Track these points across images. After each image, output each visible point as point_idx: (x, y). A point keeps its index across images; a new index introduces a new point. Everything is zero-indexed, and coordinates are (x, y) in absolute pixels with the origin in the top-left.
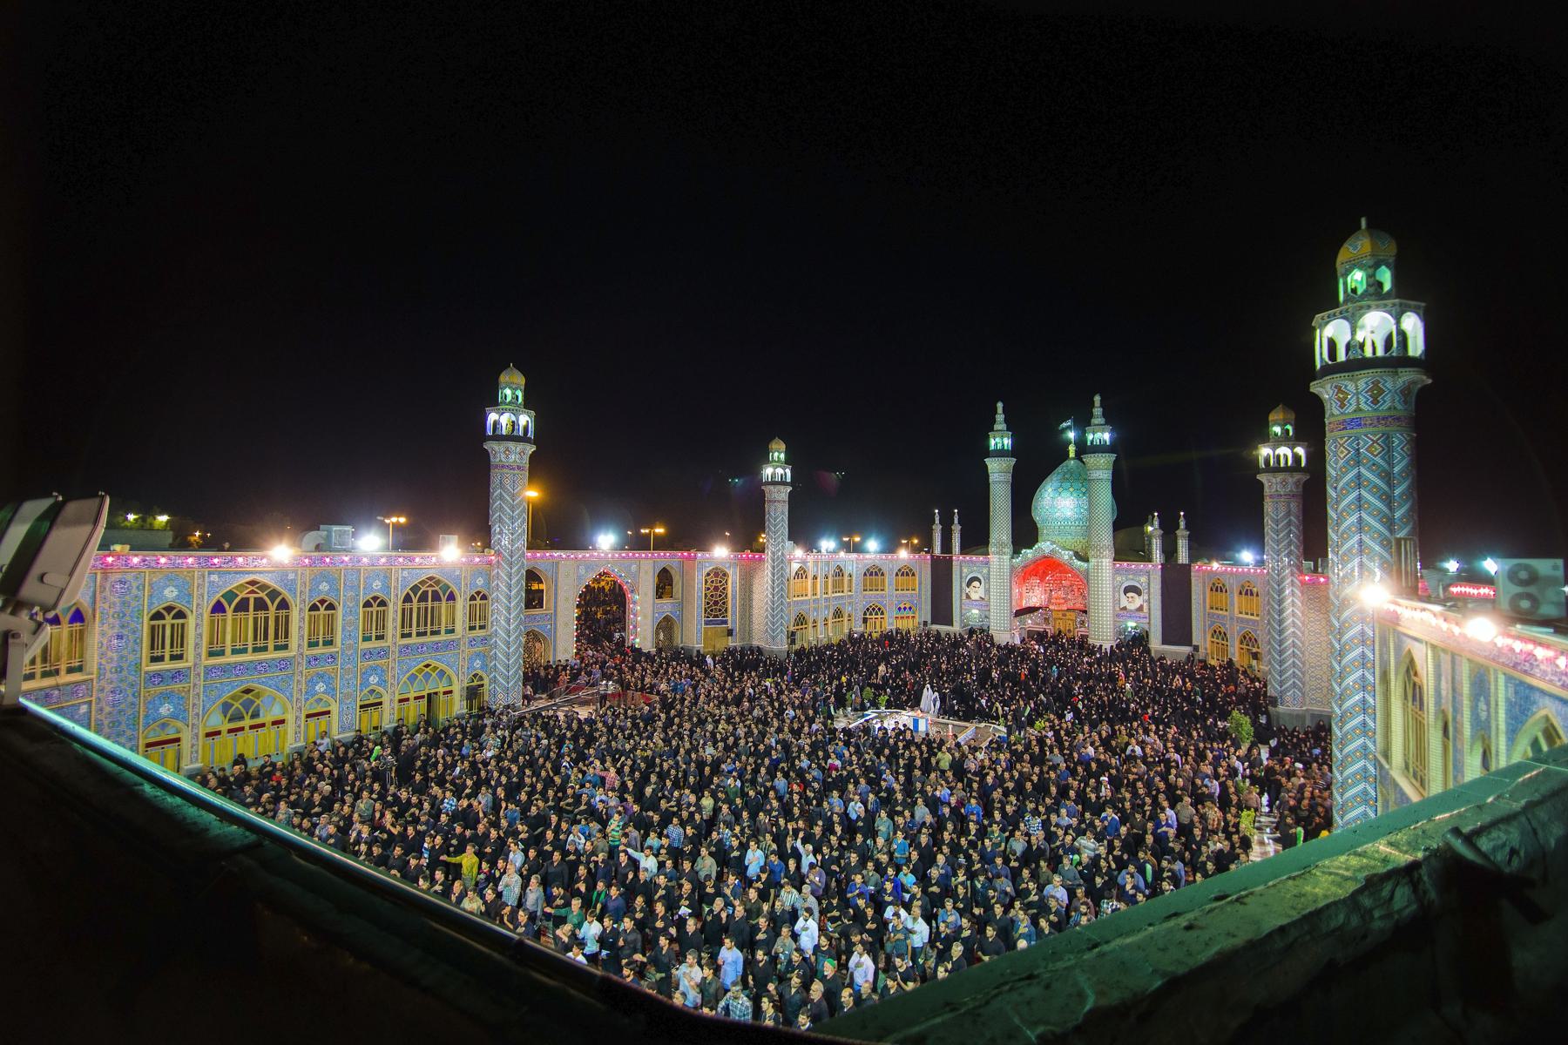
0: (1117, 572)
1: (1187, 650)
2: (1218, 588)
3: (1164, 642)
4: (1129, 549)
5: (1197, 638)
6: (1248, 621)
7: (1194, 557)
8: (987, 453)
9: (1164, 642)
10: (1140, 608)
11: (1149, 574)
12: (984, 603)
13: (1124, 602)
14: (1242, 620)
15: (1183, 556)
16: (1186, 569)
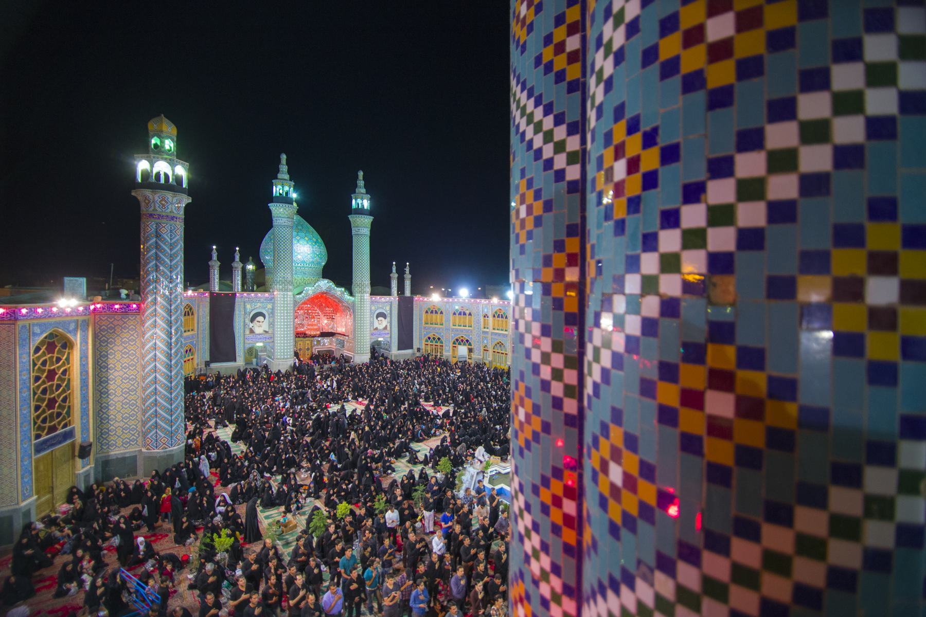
0: (372, 302)
1: (409, 351)
2: (433, 311)
3: (399, 349)
4: (380, 285)
5: (416, 344)
6: (462, 331)
7: (413, 292)
8: (271, 199)
9: (399, 349)
10: (386, 328)
11: (390, 302)
12: (269, 336)
13: (376, 325)
14: (457, 330)
15: (408, 293)
16: (410, 300)
